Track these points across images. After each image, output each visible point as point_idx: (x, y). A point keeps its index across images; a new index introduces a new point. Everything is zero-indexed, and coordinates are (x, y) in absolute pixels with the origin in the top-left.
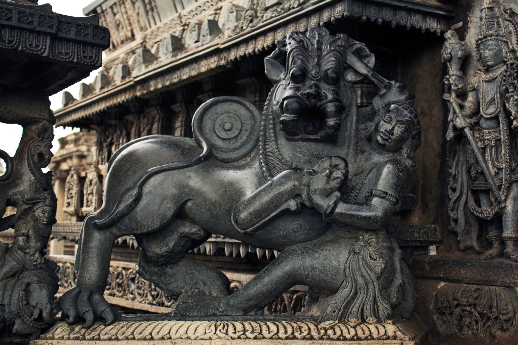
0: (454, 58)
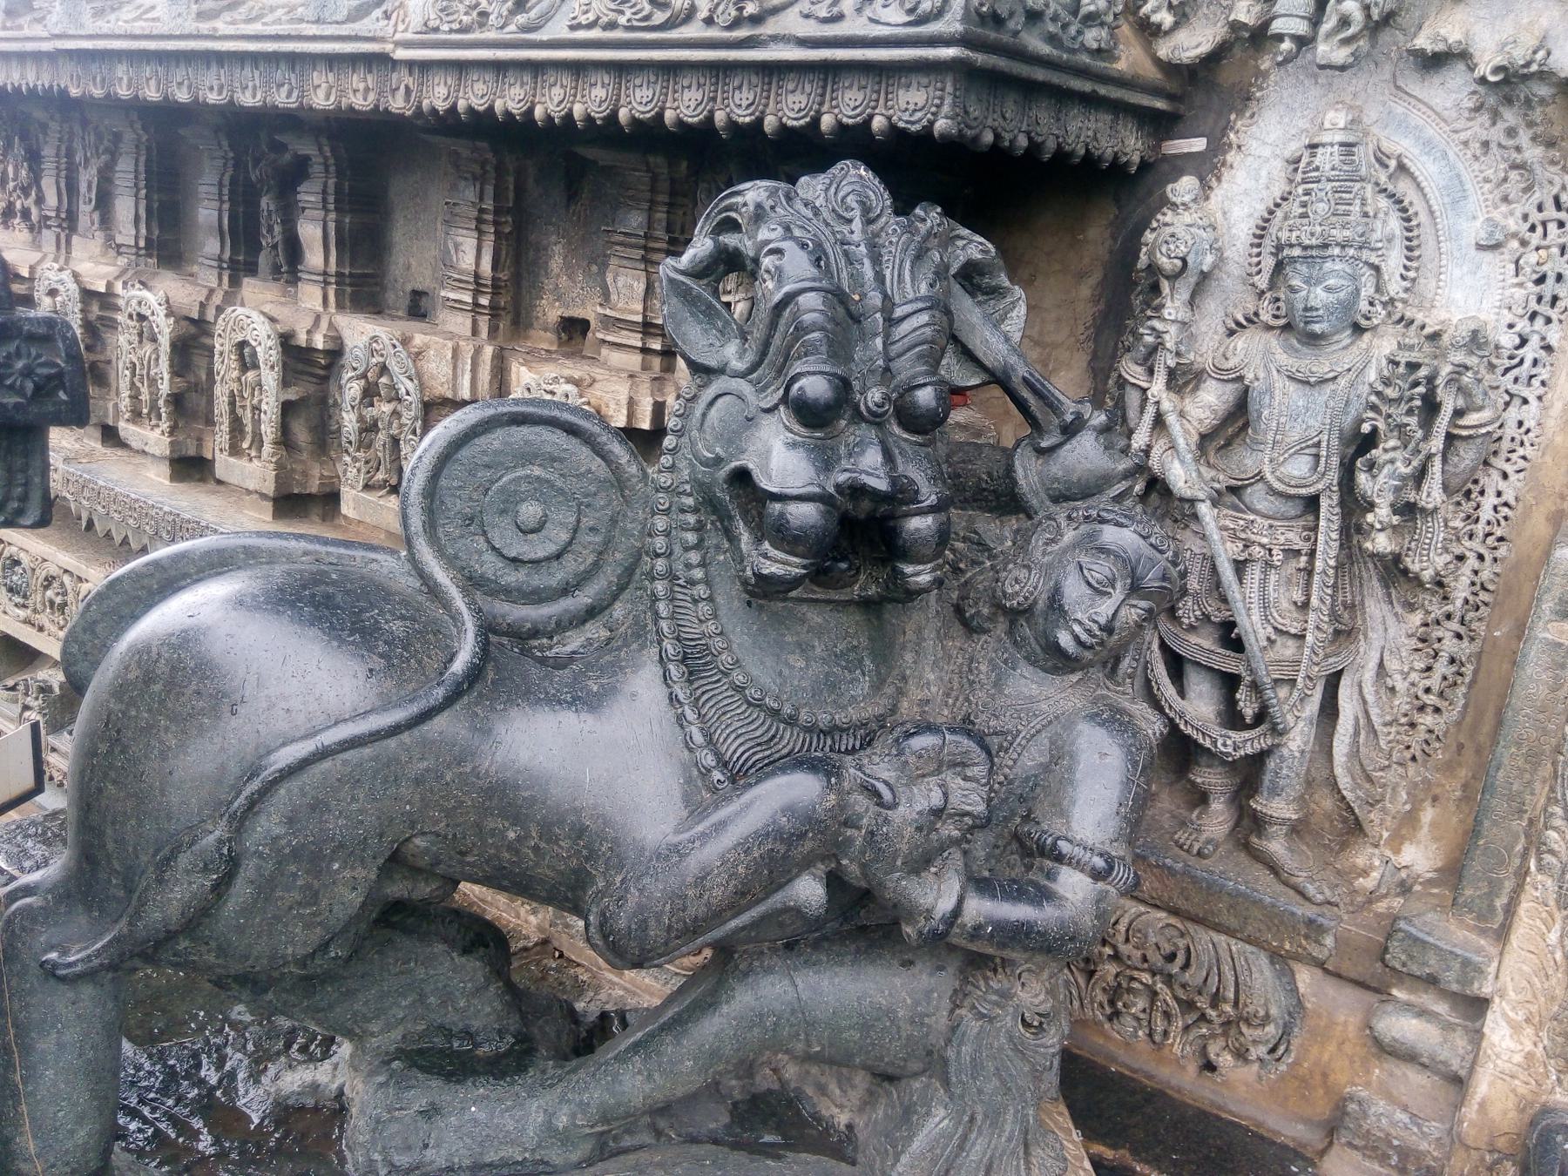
0: (1189, 272)
